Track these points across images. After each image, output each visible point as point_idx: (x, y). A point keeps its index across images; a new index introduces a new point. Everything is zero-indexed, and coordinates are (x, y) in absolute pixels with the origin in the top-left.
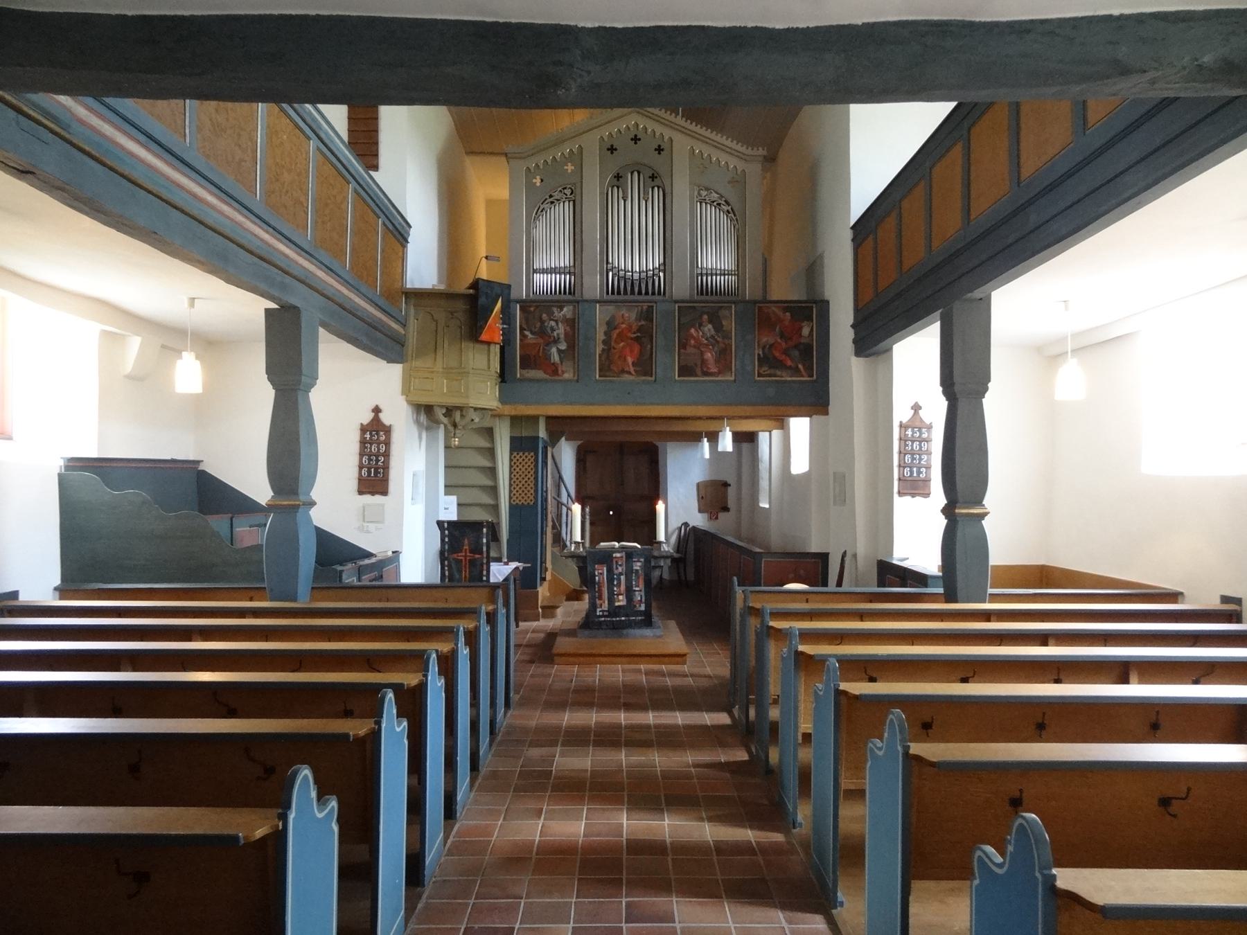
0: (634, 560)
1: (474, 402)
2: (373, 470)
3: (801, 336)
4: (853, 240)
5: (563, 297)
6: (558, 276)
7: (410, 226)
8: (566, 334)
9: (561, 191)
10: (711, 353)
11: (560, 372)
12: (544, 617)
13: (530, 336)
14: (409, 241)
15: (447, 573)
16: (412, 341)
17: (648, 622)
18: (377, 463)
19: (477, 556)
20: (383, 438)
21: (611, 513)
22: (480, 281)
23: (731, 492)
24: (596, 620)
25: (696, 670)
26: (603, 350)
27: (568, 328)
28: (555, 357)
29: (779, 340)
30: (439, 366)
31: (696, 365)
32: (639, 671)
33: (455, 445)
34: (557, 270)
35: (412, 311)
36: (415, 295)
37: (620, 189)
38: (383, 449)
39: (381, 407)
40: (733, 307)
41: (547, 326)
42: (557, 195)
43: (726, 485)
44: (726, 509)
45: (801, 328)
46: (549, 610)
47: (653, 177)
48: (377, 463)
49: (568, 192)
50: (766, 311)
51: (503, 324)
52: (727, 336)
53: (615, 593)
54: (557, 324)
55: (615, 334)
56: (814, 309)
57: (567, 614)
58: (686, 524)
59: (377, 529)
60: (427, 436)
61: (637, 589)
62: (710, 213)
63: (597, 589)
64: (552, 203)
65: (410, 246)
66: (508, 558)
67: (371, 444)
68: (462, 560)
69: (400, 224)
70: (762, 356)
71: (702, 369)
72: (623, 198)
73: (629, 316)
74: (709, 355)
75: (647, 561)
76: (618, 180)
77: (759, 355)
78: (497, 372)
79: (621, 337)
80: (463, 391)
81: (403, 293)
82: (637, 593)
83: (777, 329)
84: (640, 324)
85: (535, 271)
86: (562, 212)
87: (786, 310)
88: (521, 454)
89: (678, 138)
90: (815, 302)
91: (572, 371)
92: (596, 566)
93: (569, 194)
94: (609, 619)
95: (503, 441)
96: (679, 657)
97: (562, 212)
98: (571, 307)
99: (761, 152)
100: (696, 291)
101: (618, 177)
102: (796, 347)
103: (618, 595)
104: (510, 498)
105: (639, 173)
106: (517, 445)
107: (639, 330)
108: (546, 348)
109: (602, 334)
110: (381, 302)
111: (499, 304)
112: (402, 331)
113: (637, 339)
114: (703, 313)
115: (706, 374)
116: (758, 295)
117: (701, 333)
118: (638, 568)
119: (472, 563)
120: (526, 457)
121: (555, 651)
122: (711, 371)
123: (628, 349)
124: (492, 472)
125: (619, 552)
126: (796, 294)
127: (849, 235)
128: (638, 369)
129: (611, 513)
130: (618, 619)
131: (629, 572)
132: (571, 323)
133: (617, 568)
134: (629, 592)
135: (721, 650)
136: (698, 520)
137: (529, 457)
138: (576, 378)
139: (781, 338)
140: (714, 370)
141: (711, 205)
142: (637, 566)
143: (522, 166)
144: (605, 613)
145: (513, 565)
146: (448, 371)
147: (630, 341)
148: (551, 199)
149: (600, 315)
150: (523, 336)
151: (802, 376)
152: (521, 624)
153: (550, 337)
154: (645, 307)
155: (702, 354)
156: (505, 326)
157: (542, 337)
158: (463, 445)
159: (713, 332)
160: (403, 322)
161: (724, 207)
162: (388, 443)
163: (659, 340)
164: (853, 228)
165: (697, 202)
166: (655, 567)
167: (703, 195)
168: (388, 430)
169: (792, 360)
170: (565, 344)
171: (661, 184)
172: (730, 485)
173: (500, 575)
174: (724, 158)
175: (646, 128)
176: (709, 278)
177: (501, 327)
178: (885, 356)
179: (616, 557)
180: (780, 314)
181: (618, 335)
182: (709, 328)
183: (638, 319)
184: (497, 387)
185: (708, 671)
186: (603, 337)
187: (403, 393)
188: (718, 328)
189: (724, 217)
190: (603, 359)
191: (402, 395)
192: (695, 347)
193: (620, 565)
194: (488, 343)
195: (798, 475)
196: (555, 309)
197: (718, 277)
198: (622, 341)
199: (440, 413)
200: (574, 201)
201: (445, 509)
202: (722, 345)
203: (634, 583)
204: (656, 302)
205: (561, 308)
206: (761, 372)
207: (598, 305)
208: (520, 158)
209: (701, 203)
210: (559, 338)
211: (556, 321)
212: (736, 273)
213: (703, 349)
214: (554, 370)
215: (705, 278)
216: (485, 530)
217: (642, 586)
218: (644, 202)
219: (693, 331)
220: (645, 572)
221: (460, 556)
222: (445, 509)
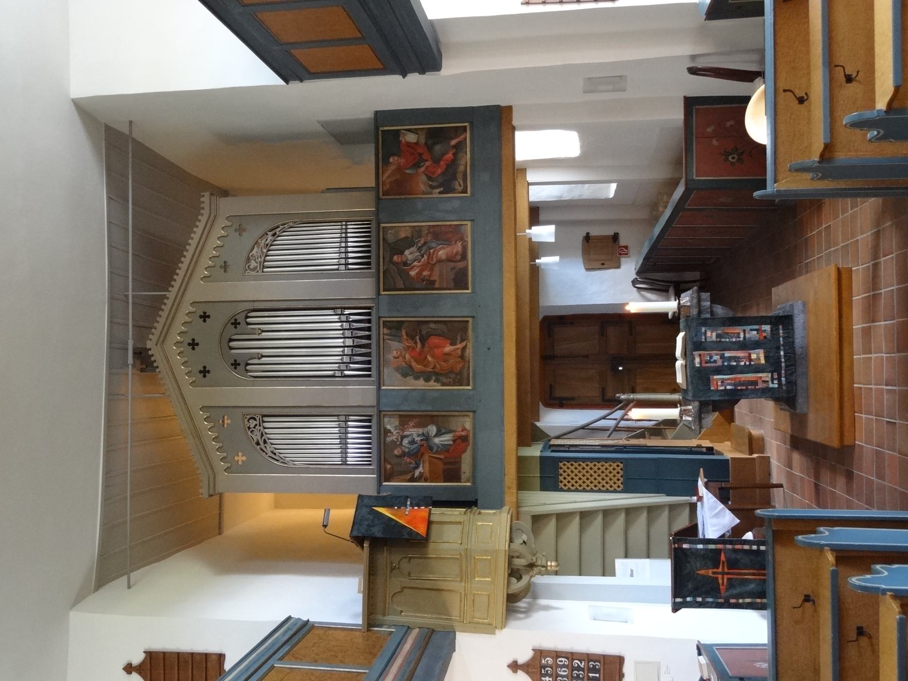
0: (703, 340)
1: (502, 544)
2: (590, 675)
3: (417, 144)
4: (301, 81)
5: (374, 430)
6: (350, 435)
7: (289, 618)
8: (418, 426)
9: (252, 432)
11: (463, 433)
12: (762, 449)
13: (421, 469)
14: (306, 619)
15: (748, 600)
16: (428, 620)
17: (785, 321)
18: (583, 670)
19: (723, 557)
20: (550, 660)
21: (621, 368)
22: (355, 533)
23: (595, 232)
24: (784, 388)
25: (864, 252)
26: (437, 381)
27: (411, 424)
28: (446, 439)
29: (423, 169)
30: (458, 586)
32: (866, 332)
33: (556, 566)
34: (343, 436)
35: (389, 618)
36: (372, 613)
37: (250, 362)
38: (563, 661)
39: (510, 661)
40: (383, 225)
42: (256, 436)
43: (587, 238)
44: (615, 237)
45: (409, 145)
46: (754, 444)
47: (236, 324)
48: (583, 670)
49: (253, 423)
50: (388, 186)
51: (406, 506)
52: (418, 231)
53: (748, 363)
54: (407, 436)
55: (418, 367)
56: (385, 128)
57: (759, 422)
58: (634, 282)
59: (668, 672)
60: (546, 599)
61: (742, 335)
62: (276, 256)
63: (744, 388)
64: (265, 442)
65: (313, 619)
66: (691, 496)
67: (557, 676)
68: (728, 579)
69: (286, 632)
70: (442, 189)
72: (259, 359)
73: (395, 349)
74: (440, 253)
75: (705, 323)
76: (239, 364)
77: (440, 193)
78: (467, 510)
79: (422, 360)
80: (489, 557)
81: (368, 630)
82: (747, 335)
83: (408, 171)
84: (405, 337)
85: (344, 463)
86: (276, 430)
87: (386, 162)
88: (561, 478)
89: (190, 297)
90: (377, 128)
91: (461, 419)
92: (712, 388)
93: (255, 422)
94: (783, 372)
95: (547, 503)
96: (842, 279)
97: (276, 430)
98: (386, 420)
99: (206, 198)
100: (366, 271)
101: (235, 365)
102: (430, 149)
103: (750, 360)
104: (615, 491)
105: (231, 340)
106: (550, 482)
107: (413, 338)
109: (417, 382)
110: (379, 665)
112: (415, 632)
113: (423, 340)
115: (464, 257)
116: (371, 196)
117: (416, 263)
118: (714, 334)
119: (733, 564)
121: (835, 443)
122: (460, 249)
123: (436, 351)
124: (585, 515)
125: (694, 359)
126: (368, 154)
127: (295, 86)
128: (459, 337)
129: (621, 368)
130: (783, 360)
131: (720, 346)
132: (405, 419)
133: (715, 362)
134: (745, 345)
135: (820, 224)
136: (629, 268)
137: (565, 468)
138: (471, 414)
139: (420, 167)
140: (458, 247)
141: (267, 256)
142: (711, 335)
143: (223, 478)
144: (776, 376)
145: (702, 490)
146: (464, 576)
148: (261, 443)
149: (395, 384)
151: (465, 139)
152: (775, 480)
153: (422, 446)
154: (386, 331)
155: (440, 261)
156: (409, 503)
157: (422, 454)
158: (553, 554)
159: (413, 249)
160: (405, 629)
161: (269, 240)
162: (557, 654)
163: (425, 313)
164: (287, 81)
165: (263, 272)
166: (712, 313)
167: (256, 264)
168: (540, 653)
169: (447, 153)
170: (429, 427)
171: (244, 314)
172: (588, 233)
173: (716, 508)
174: (214, 241)
175: (181, 332)
176: (350, 255)
177: (409, 508)
178: (438, 29)
179: (701, 363)
180: (392, 168)
181: (417, 361)
182: (410, 254)
183: (399, 339)
184: (483, 511)
185: (864, 237)
187: (494, 634)
188: (408, 243)
189: (281, 240)
191: (494, 634)
192: (432, 270)
193: (711, 357)
194: (430, 523)
195: (582, 147)
196: (389, 439)
197: (350, 244)
198: (426, 357)
199: (517, 586)
200: (264, 416)
201: (632, 575)
203: (734, 340)
204: (379, 318)
205: (387, 432)
206: (460, 189)
207: (383, 388)
208: (214, 478)
209: (264, 267)
210: (423, 434)
211: (403, 437)
212: (344, 223)
214: (462, 440)
215: (351, 261)
216: (685, 546)
217: (738, 329)
218: (264, 334)
219: (413, 273)
220: (721, 326)
221: (723, 581)
222: (632, 575)
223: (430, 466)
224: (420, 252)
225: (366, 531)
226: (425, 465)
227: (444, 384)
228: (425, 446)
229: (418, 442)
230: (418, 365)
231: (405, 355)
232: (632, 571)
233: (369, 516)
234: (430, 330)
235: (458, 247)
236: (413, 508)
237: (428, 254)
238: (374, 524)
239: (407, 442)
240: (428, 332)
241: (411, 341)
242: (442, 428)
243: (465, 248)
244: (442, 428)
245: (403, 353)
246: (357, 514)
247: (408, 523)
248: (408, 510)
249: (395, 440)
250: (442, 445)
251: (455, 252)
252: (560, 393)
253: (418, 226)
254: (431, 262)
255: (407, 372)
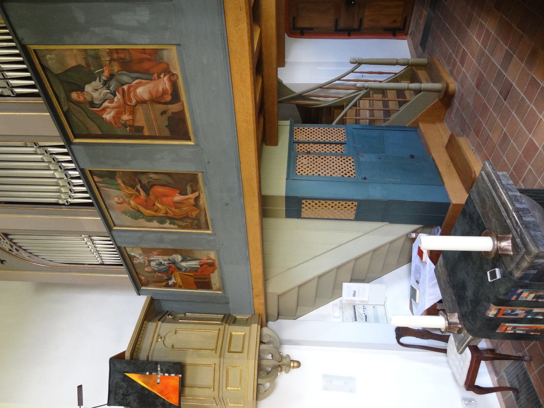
10: (136, 88)
31: (164, 113)
41: (159, 268)
51: (157, 371)
54: (153, 260)
55: (148, 212)
71: (171, 103)
74: (140, 90)
84: (122, 185)
88: (303, 206)
107: (133, 187)
108: (183, 271)
111: (133, 376)
114: (69, 99)
115: (176, 97)
117: (106, 104)
120: (306, 206)
123: (165, 199)
137: (307, 204)
140: (164, 83)
147: (152, 197)
150: (174, 285)
155: (142, 102)
156: (159, 369)
157: (172, 273)
159: (96, 84)
181: (146, 208)
186: (155, 224)
190: (181, 223)
192: (133, 113)
198: (154, 205)
201: (354, 295)
202: (116, 68)
213: (134, 101)
222: (354, 295)
223: (181, 278)
224: (108, 88)
225: (123, 399)
226: (177, 278)
227: (181, 227)
228: (173, 267)
229: (166, 264)
230: (146, 210)
231: (129, 202)
232: (355, 292)
233: (123, 383)
234: (150, 180)
235: (164, 83)
236: (164, 375)
237: (121, 93)
238: (128, 393)
239: (155, 264)
240: (149, 182)
241: (131, 189)
242: (187, 257)
243: (174, 85)
244: (187, 257)
245: (127, 200)
246: (111, 382)
247: (160, 393)
248: (159, 376)
249: (143, 262)
250: (190, 267)
251: (161, 89)
252: (302, 24)
253: (94, 50)
254: (129, 104)
255: (137, 215)
